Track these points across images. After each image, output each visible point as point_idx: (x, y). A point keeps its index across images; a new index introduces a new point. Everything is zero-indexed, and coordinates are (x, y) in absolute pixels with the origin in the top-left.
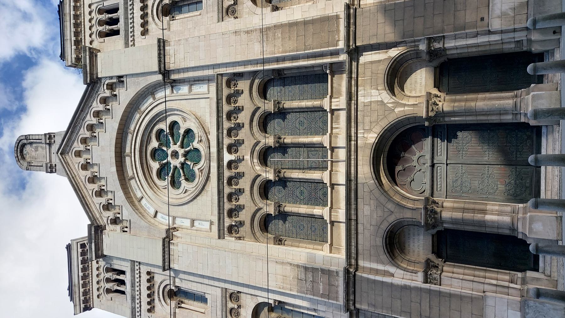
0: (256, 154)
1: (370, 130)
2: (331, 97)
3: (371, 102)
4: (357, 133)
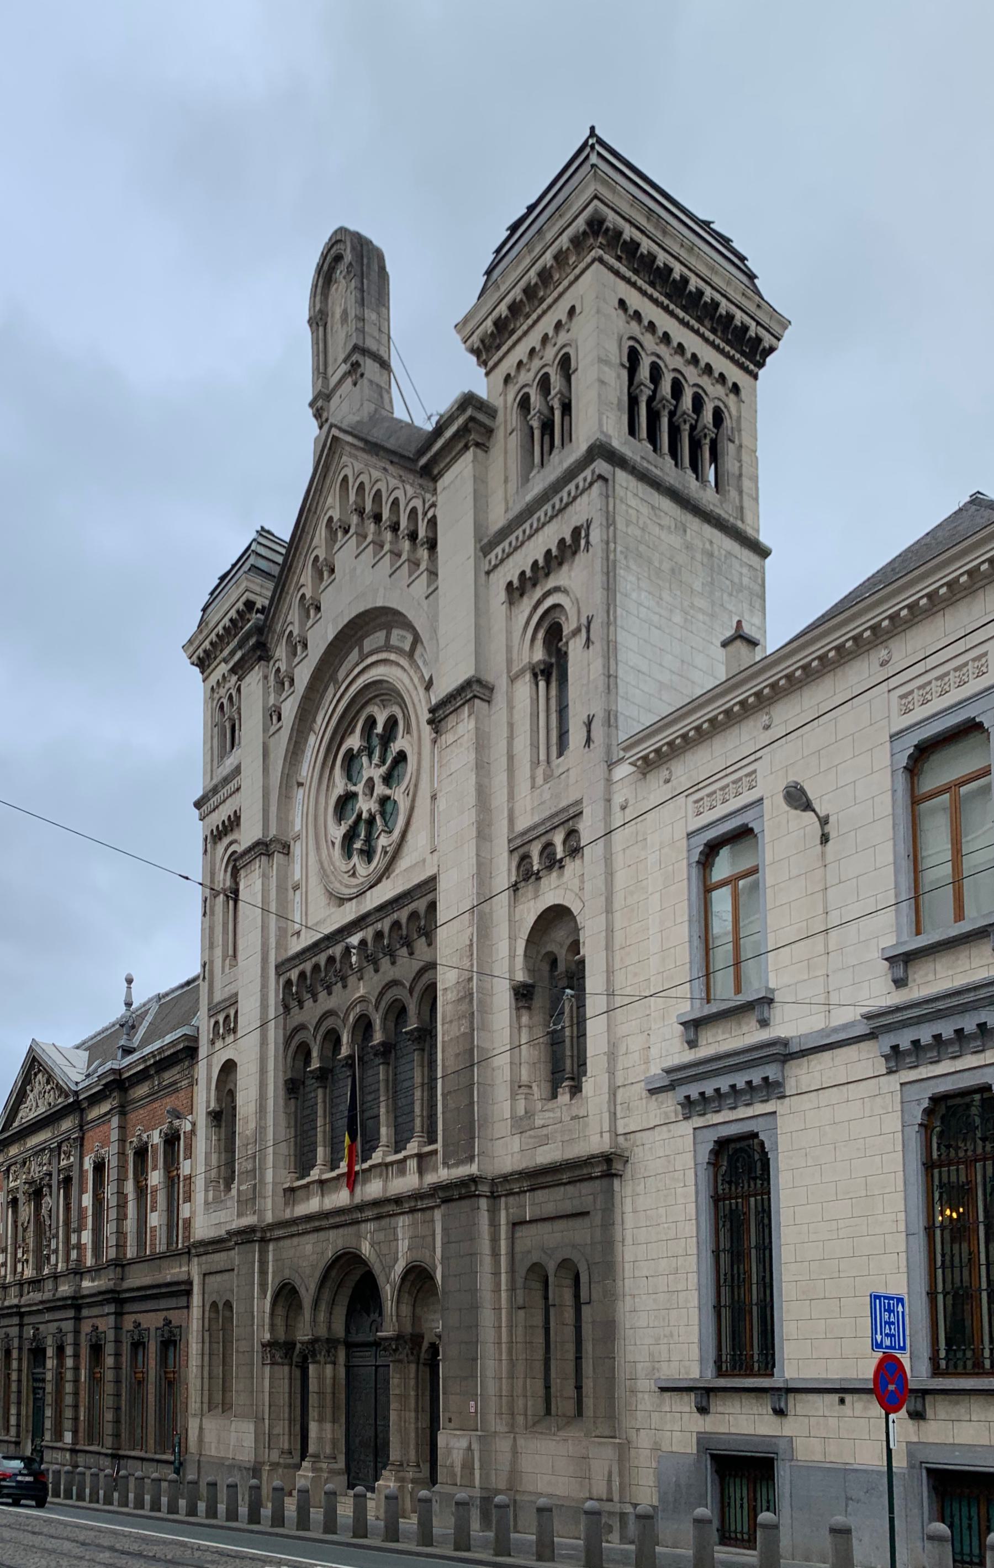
3: (397, 1240)
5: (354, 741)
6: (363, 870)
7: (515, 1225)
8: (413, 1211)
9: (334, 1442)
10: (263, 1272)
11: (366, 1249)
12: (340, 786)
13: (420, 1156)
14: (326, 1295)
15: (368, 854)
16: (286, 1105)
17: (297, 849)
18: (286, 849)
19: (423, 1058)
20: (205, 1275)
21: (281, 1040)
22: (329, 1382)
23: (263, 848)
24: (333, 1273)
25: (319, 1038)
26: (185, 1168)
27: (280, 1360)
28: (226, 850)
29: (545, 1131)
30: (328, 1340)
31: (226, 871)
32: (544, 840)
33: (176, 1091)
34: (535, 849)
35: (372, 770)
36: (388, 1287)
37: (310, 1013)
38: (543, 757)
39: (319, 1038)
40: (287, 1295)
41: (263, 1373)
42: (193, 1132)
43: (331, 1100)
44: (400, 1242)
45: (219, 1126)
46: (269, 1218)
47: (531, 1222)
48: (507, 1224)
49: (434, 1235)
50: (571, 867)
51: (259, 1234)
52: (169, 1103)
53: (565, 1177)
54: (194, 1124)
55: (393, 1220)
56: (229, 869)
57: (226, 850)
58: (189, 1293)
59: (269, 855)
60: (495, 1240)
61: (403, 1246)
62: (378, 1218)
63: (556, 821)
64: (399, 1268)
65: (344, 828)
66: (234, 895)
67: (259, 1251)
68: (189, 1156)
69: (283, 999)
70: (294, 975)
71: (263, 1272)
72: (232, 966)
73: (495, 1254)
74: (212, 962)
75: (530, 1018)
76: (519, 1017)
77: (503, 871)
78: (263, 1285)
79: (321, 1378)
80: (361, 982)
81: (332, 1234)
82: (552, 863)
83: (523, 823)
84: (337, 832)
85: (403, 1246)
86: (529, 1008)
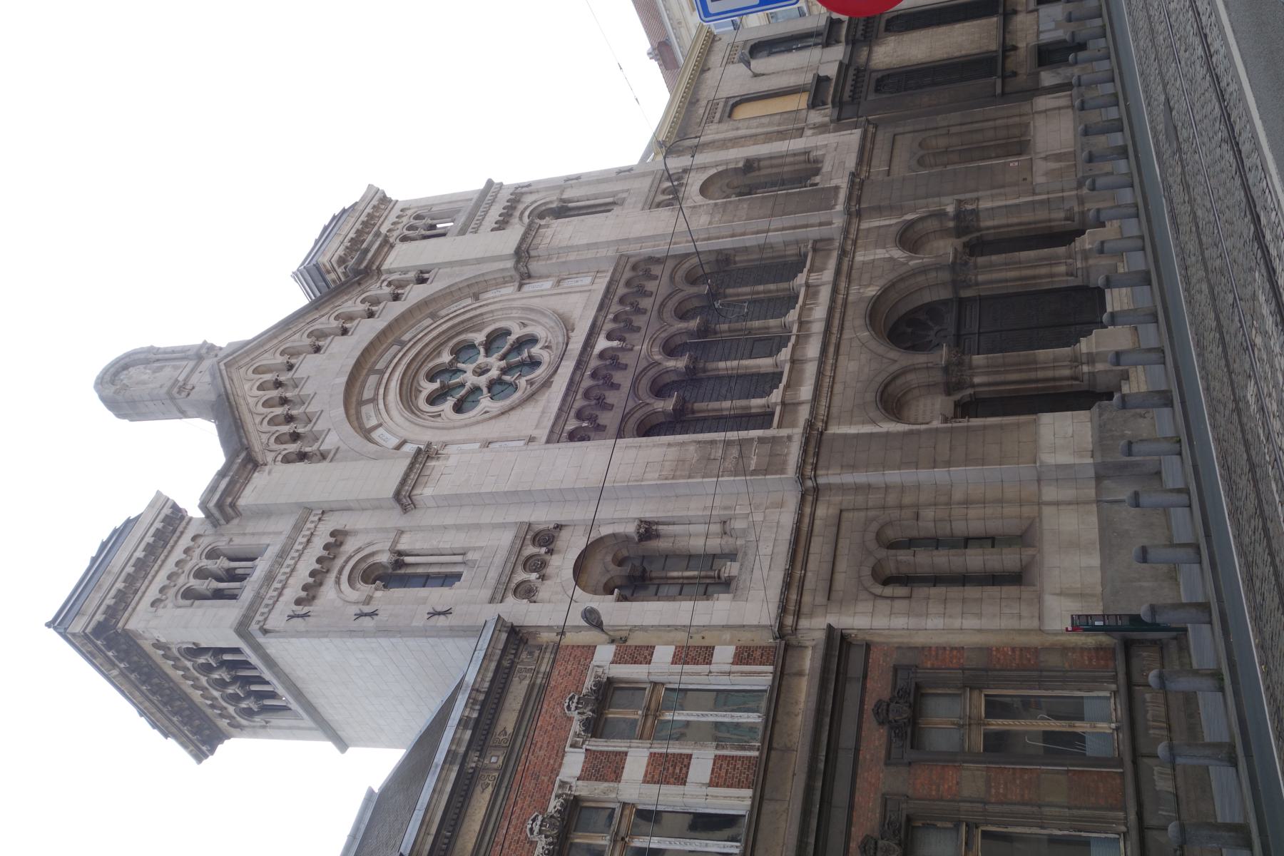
0: (658, 342)
2: (810, 271)
4: (848, 289)
8: (855, 243)
36: (911, 263)
49: (879, 227)
53: (868, 145)
55: (856, 266)
85: (881, 253)
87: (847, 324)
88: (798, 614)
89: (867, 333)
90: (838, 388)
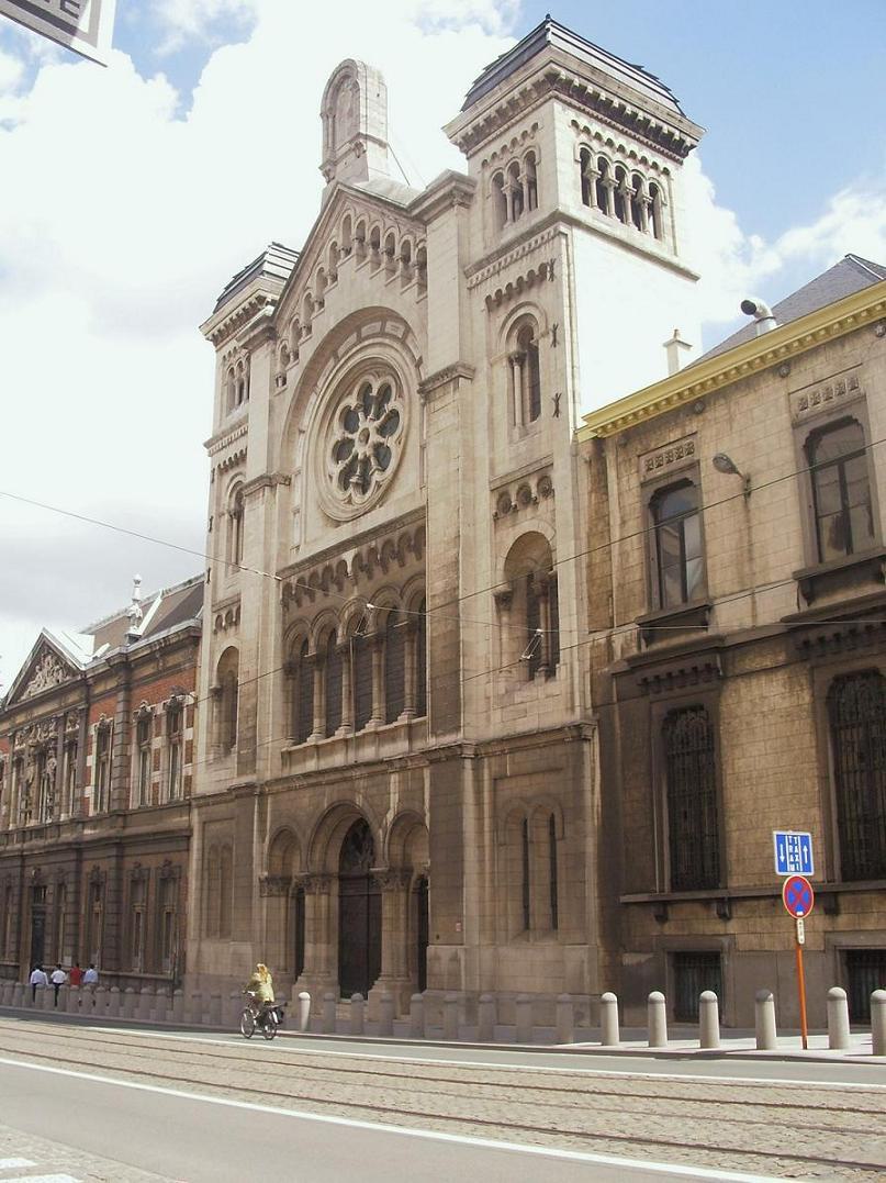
1: (365, 798)
5: (352, 401)
6: (358, 498)
7: (495, 780)
9: (328, 960)
10: (262, 821)
11: (359, 800)
12: (338, 433)
13: (410, 726)
14: (322, 838)
15: (363, 486)
16: (284, 685)
17: (298, 483)
18: (288, 481)
19: (412, 647)
20: (205, 823)
21: (280, 631)
22: (323, 910)
23: (267, 482)
24: (329, 821)
25: (315, 631)
26: (188, 734)
27: (277, 893)
28: (232, 480)
29: (522, 706)
30: (323, 875)
31: (230, 496)
32: (521, 482)
33: (181, 671)
34: (513, 491)
35: (367, 424)
37: (309, 608)
38: (518, 420)
39: (315, 631)
40: (283, 838)
41: (261, 904)
42: (195, 705)
43: (327, 680)
44: (392, 795)
45: (220, 701)
46: (268, 776)
47: (511, 777)
48: (490, 779)
49: (423, 788)
50: (544, 505)
51: (258, 790)
52: (174, 681)
54: (196, 699)
56: (234, 495)
57: (232, 480)
58: (189, 838)
59: (272, 487)
60: (478, 792)
61: (394, 799)
62: (371, 775)
63: (531, 469)
64: (390, 816)
65: (342, 465)
66: (238, 515)
67: (259, 804)
68: (191, 724)
69: (283, 600)
70: (294, 580)
71: (262, 821)
72: (234, 572)
73: (479, 803)
74: (216, 569)
75: (510, 618)
76: (499, 618)
77: (486, 504)
78: (262, 832)
79: (316, 907)
80: (356, 588)
81: (328, 789)
82: (527, 499)
83: (501, 470)
84: (336, 469)
85: (394, 799)
86: (509, 610)
87: (336, 786)
88: (199, 807)
89: (326, 805)
90: (293, 794)
